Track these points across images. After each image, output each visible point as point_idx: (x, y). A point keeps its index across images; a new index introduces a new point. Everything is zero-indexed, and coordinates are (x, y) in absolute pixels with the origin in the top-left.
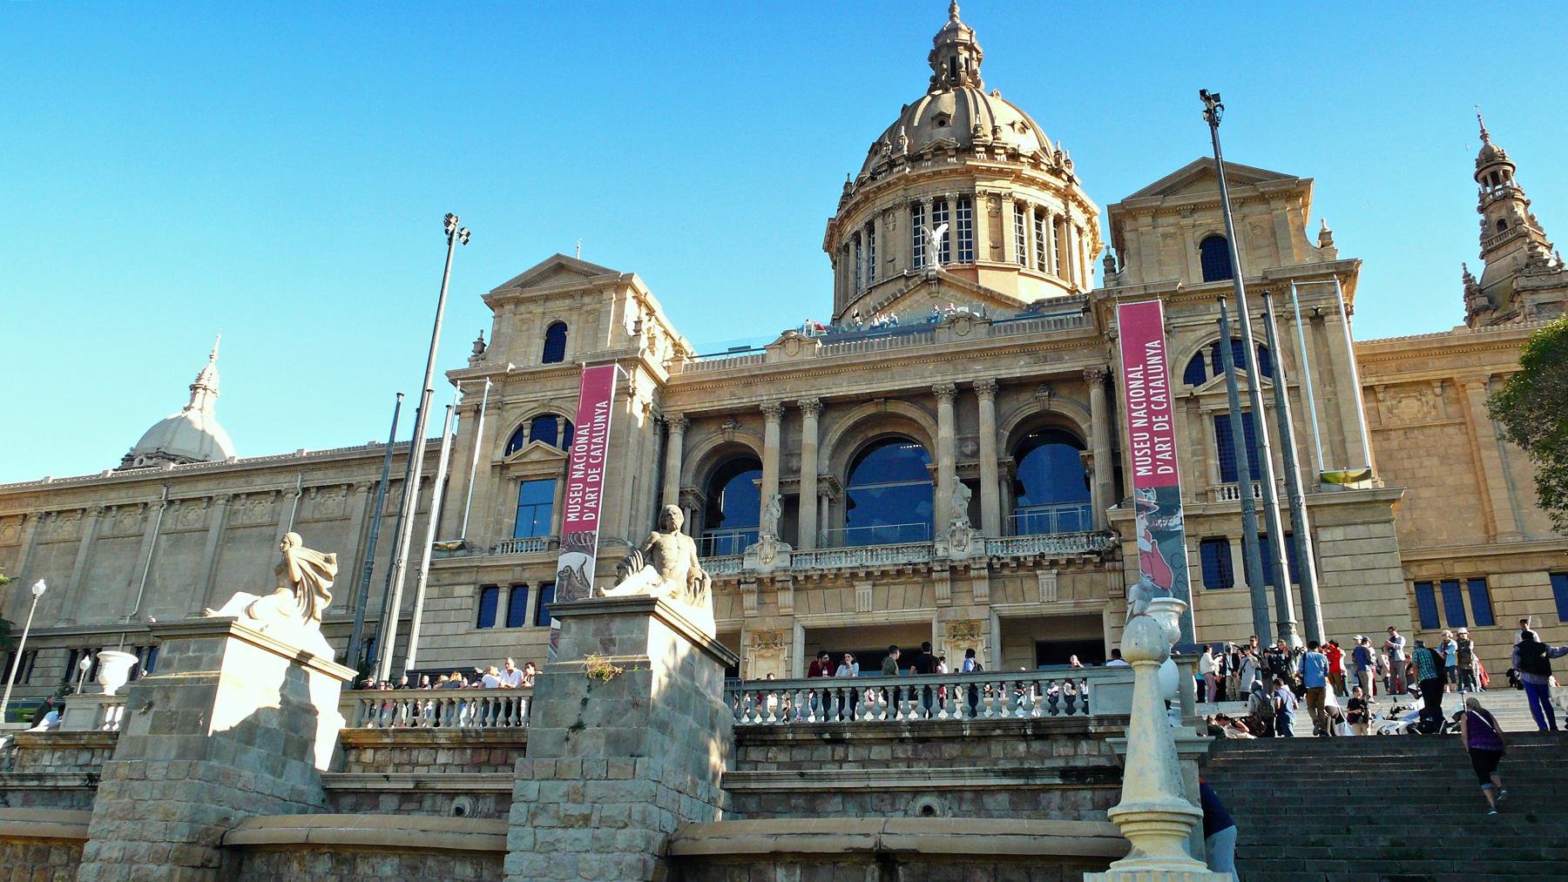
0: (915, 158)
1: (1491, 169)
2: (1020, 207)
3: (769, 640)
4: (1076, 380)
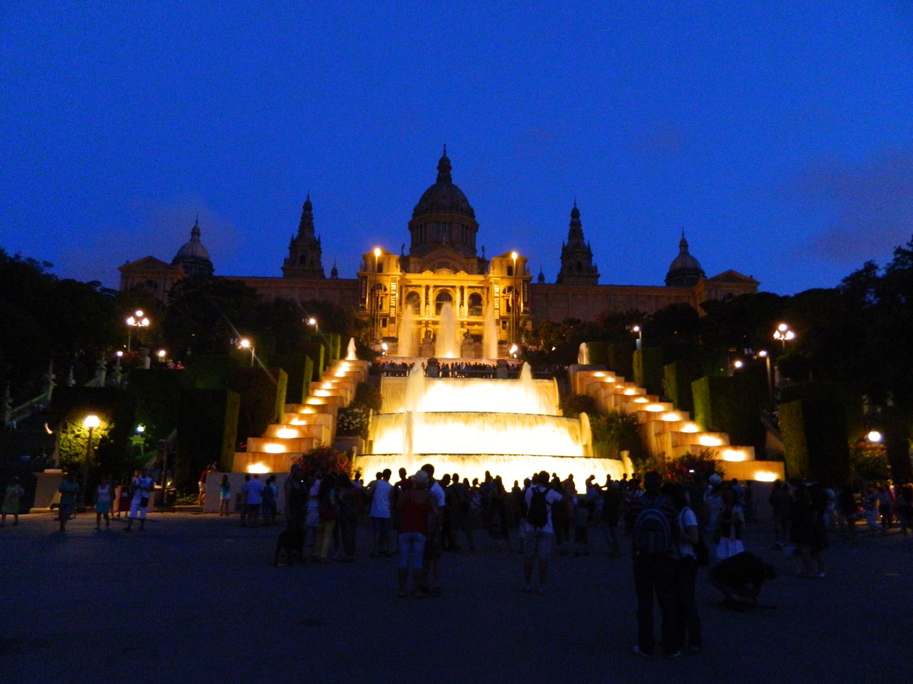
1: (575, 214)
2: (463, 226)
4: (482, 288)
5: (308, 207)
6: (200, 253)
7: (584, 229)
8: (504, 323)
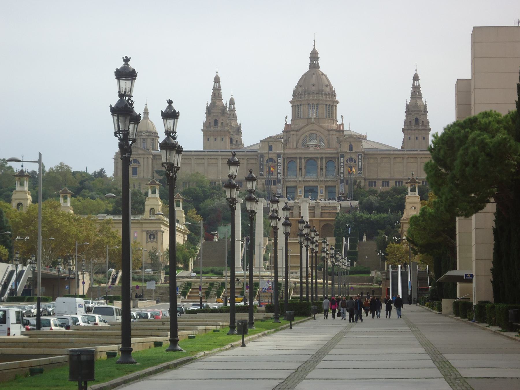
0: (309, 94)
1: (416, 78)
2: (326, 105)
3: (300, 187)
4: (334, 157)
5: (217, 80)
6: (151, 129)
7: (423, 90)
8: (347, 181)
